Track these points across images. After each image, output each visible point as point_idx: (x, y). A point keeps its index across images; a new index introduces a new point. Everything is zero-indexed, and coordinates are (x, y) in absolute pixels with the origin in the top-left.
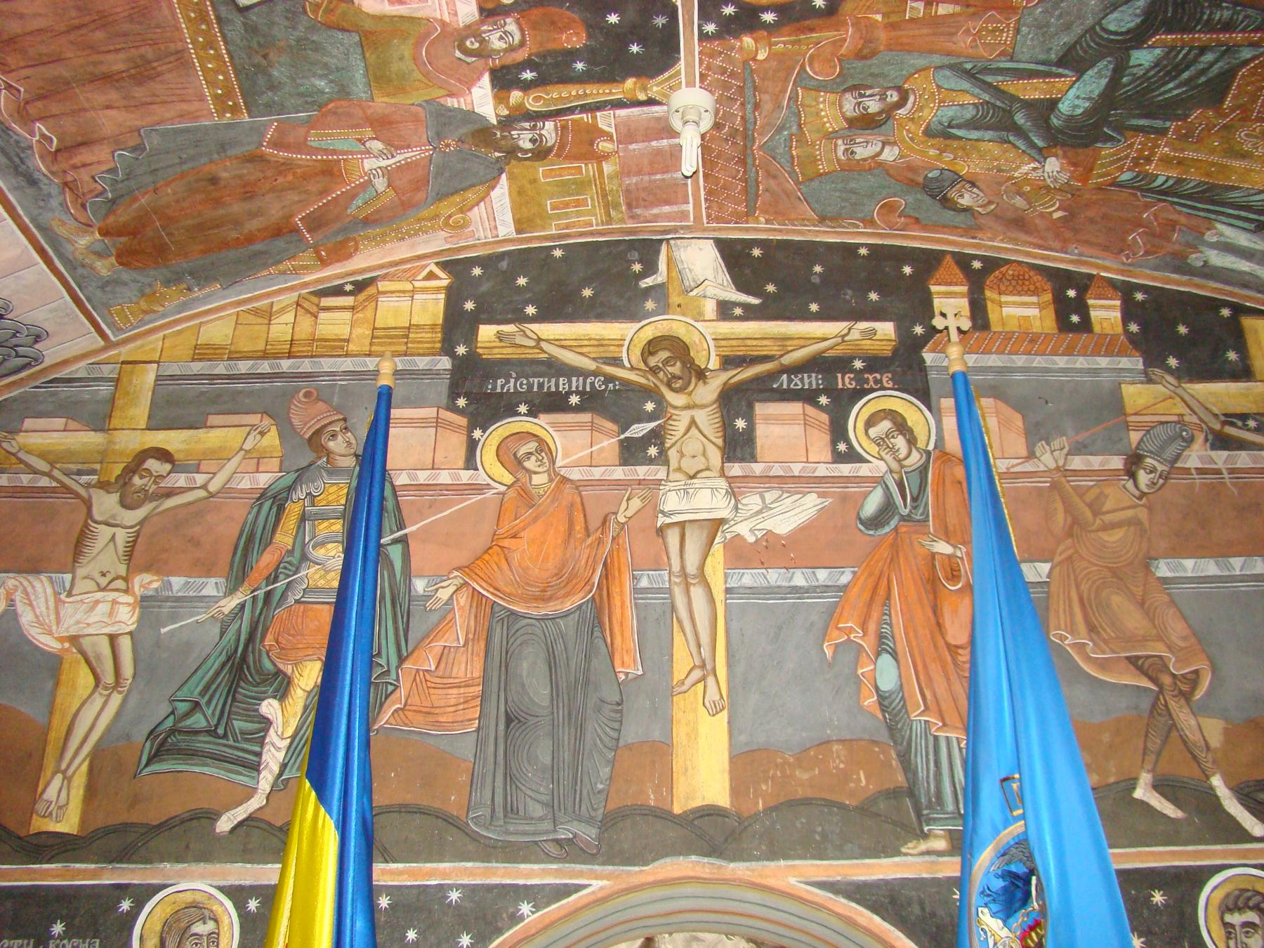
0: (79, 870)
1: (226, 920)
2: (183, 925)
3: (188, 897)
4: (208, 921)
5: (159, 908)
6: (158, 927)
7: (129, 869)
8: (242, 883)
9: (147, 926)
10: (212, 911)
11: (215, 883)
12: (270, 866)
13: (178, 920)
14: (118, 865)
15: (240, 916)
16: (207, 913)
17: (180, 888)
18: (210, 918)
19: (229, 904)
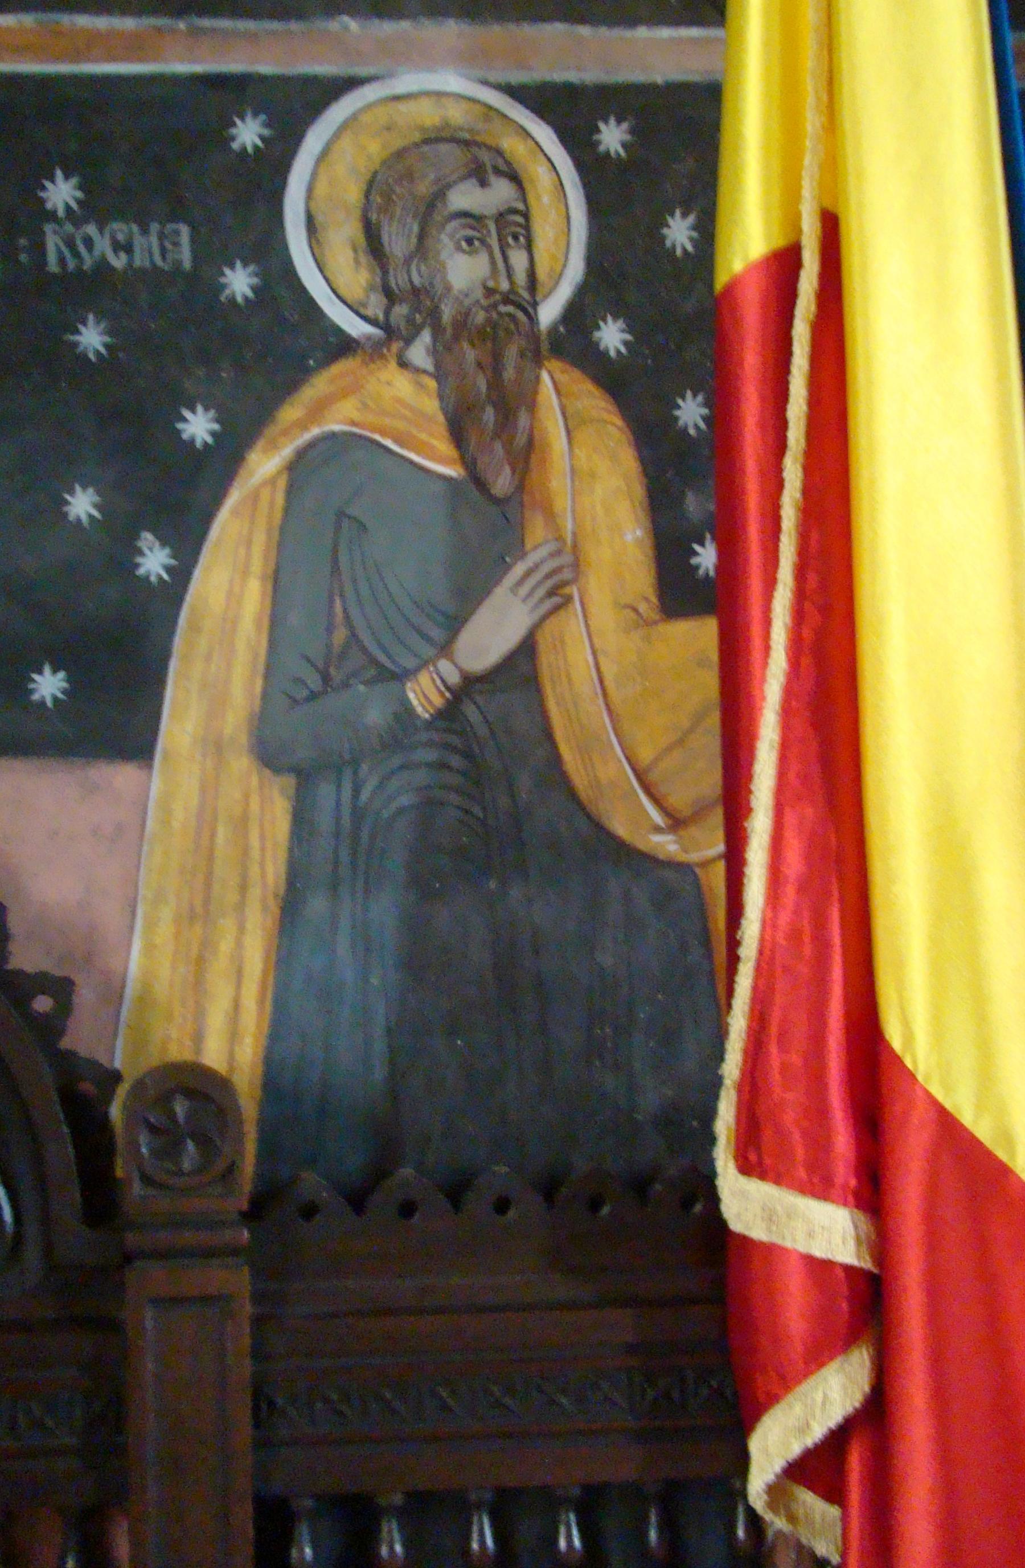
0: (94, 37)
1: (540, 177)
2: (424, 188)
3: (428, 115)
4: (493, 179)
5: (346, 143)
6: (353, 193)
7: (235, 34)
8: (572, 76)
9: (322, 189)
10: (499, 152)
11: (494, 77)
12: (642, 32)
13: (409, 176)
14: (206, 23)
15: (580, 165)
16: (485, 157)
17: (407, 82)
18: (498, 172)
19: (544, 134)
